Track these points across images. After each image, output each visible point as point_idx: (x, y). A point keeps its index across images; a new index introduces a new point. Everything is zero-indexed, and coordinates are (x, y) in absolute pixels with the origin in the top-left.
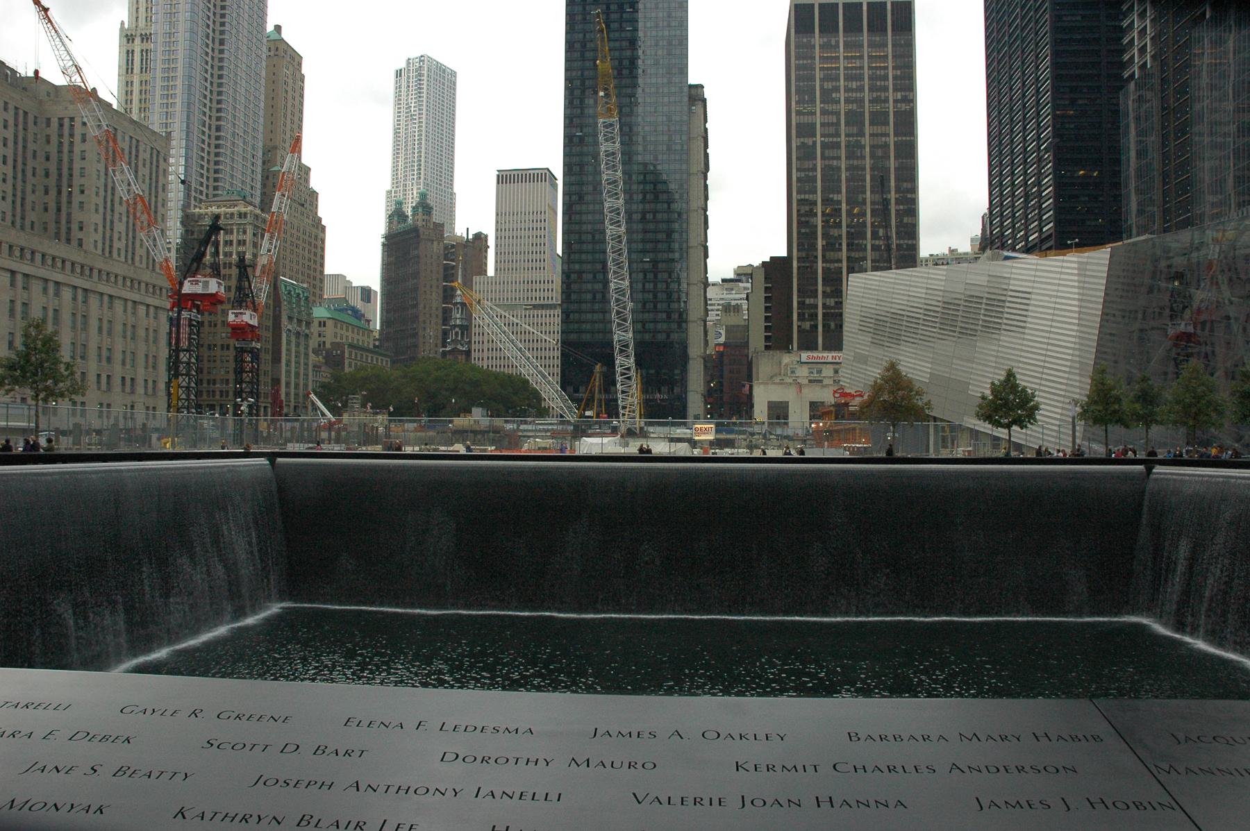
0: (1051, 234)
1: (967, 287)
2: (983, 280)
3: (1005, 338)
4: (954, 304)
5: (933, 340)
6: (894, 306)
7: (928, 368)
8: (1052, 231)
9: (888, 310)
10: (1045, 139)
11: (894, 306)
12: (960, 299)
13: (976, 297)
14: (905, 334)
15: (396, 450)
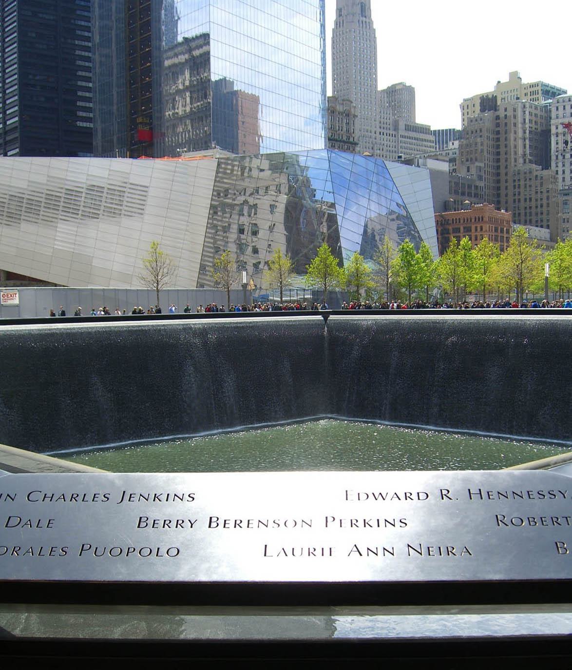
0: (17, 127)
1: (90, 178)
2: (106, 174)
3: (125, 221)
4: (76, 191)
5: (53, 220)
6: (13, 189)
7: (58, 245)
8: (17, 124)
9: (6, 192)
10: (10, 43)
11: (13, 189)
12: (83, 188)
13: (98, 186)
14: (26, 214)
15: (267, 310)
